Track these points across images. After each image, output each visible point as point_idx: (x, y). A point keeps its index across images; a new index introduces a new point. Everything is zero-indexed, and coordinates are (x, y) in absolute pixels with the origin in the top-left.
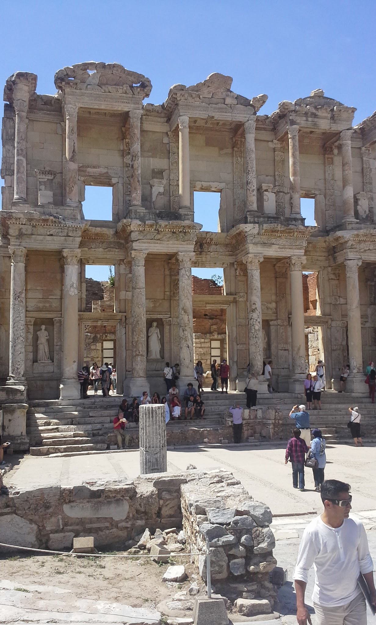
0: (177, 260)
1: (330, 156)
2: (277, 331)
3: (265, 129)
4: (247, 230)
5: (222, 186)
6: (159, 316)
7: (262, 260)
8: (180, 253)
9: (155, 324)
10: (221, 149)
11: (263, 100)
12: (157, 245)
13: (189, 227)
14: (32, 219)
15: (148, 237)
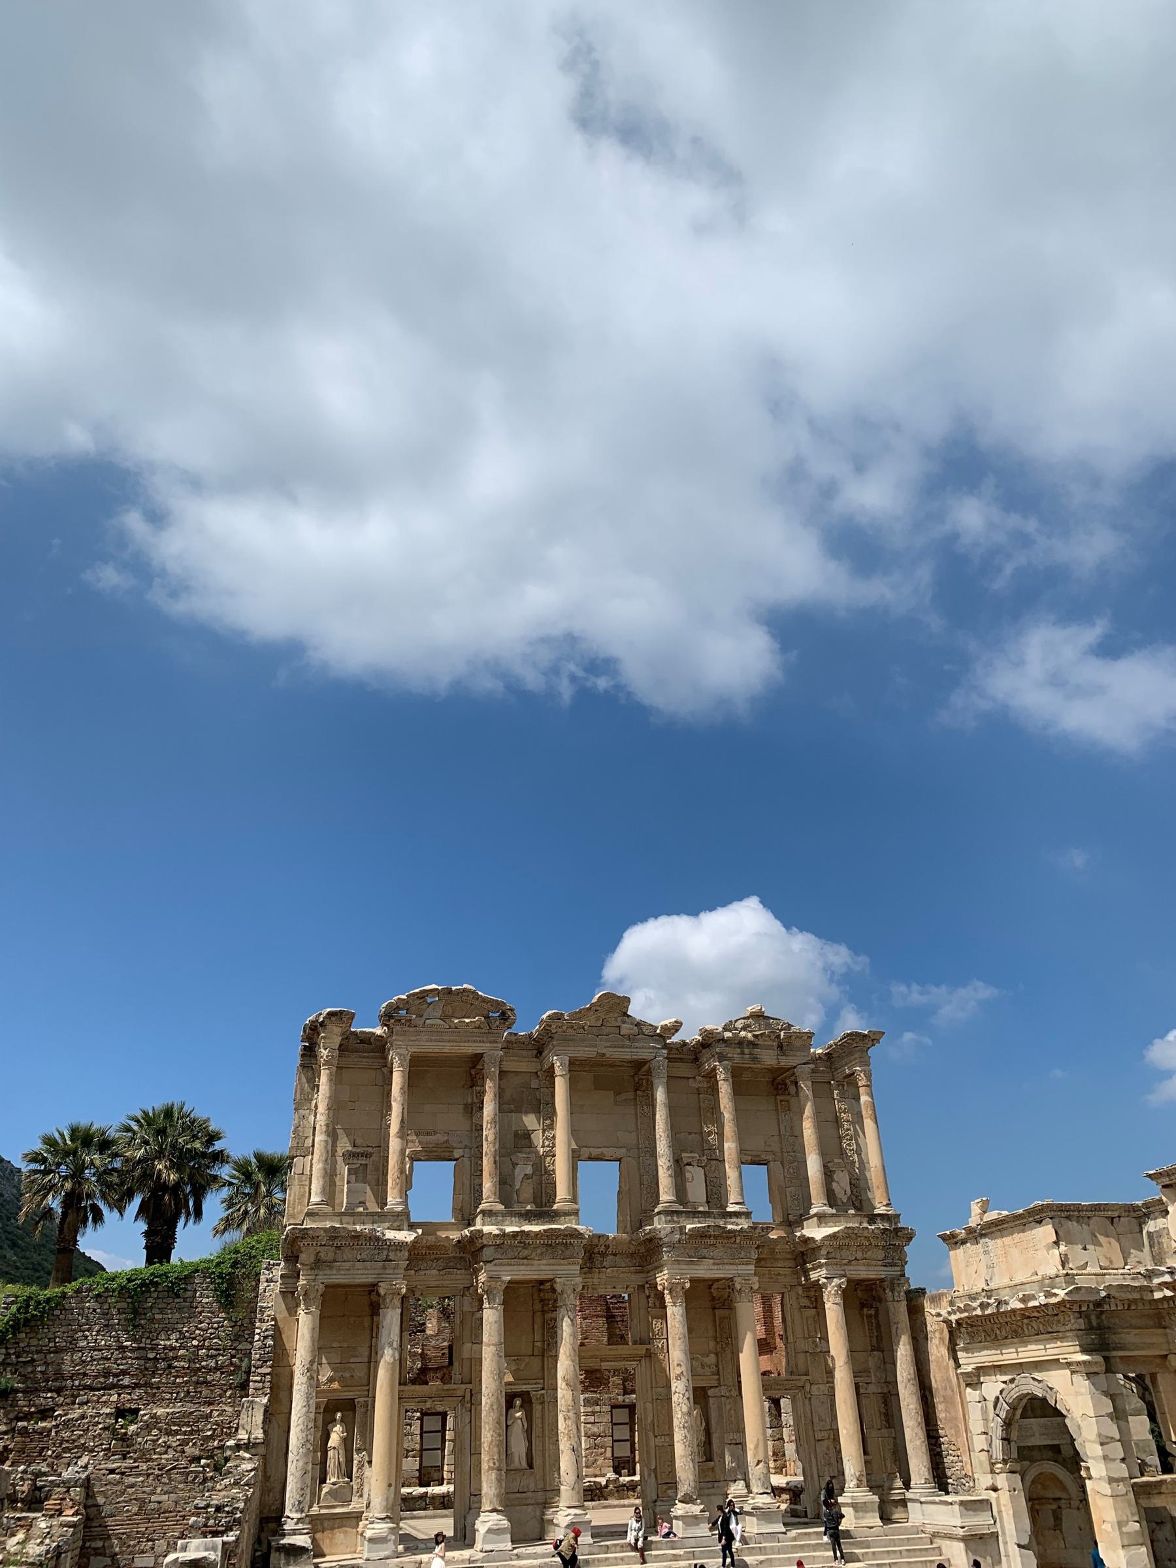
0: (553, 1290)
1: (782, 1098)
2: (720, 1408)
3: (681, 1060)
4: (662, 1235)
5: (621, 1152)
6: (524, 1388)
7: (688, 1285)
8: (558, 1280)
9: (518, 1402)
10: (617, 1093)
11: (676, 1027)
12: (522, 1268)
13: (572, 1236)
14: (336, 1237)
15: (510, 1254)
